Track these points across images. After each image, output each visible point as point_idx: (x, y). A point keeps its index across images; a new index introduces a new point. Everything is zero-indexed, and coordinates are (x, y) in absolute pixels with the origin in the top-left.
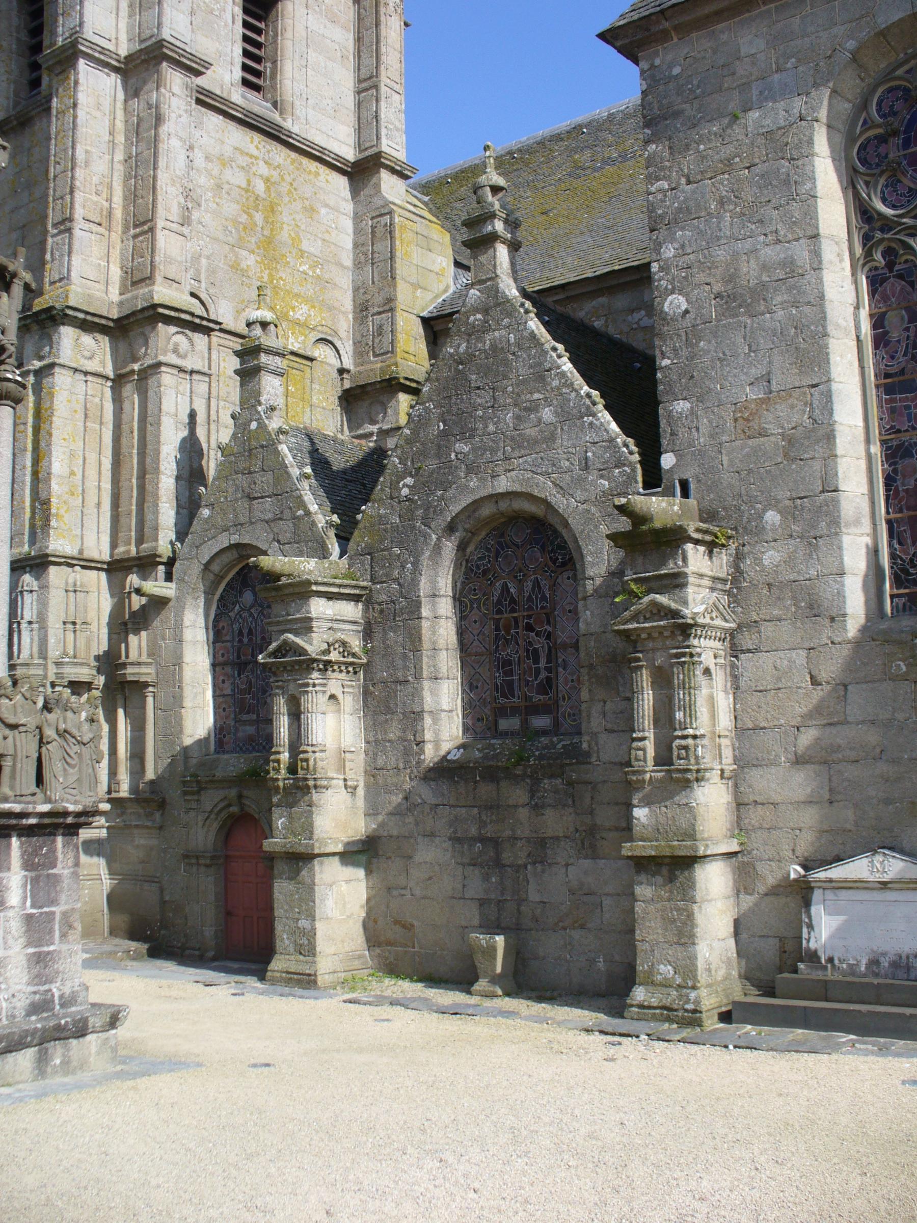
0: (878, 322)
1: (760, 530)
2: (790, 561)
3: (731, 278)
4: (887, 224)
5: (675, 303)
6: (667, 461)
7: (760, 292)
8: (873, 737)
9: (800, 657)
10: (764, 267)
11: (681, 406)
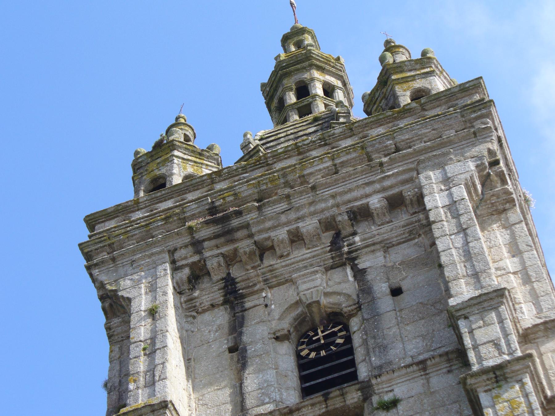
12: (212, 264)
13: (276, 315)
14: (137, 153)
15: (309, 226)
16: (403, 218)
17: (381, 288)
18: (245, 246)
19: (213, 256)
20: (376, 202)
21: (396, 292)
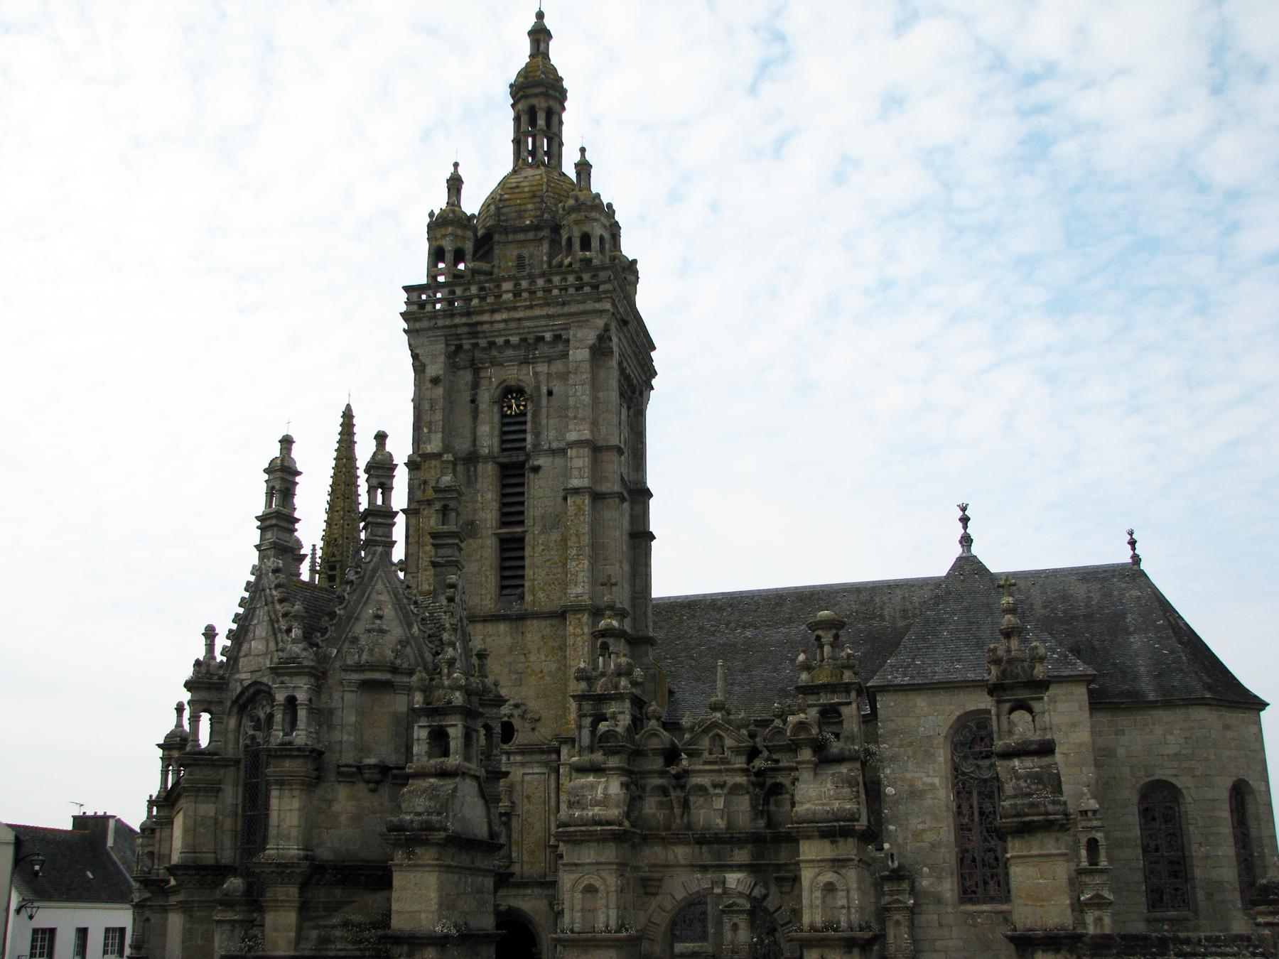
0: (959, 807)
1: (921, 874)
2: (932, 885)
3: (911, 786)
4: (963, 774)
5: (890, 790)
6: (886, 846)
7: (923, 792)
8: (961, 944)
9: (936, 917)
10: (924, 784)
11: (892, 827)
12: (466, 347)
13: (494, 385)
14: (431, 215)
15: (514, 340)
16: (561, 347)
17: (544, 390)
18: (483, 343)
19: (467, 344)
20: (548, 336)
21: (550, 393)
